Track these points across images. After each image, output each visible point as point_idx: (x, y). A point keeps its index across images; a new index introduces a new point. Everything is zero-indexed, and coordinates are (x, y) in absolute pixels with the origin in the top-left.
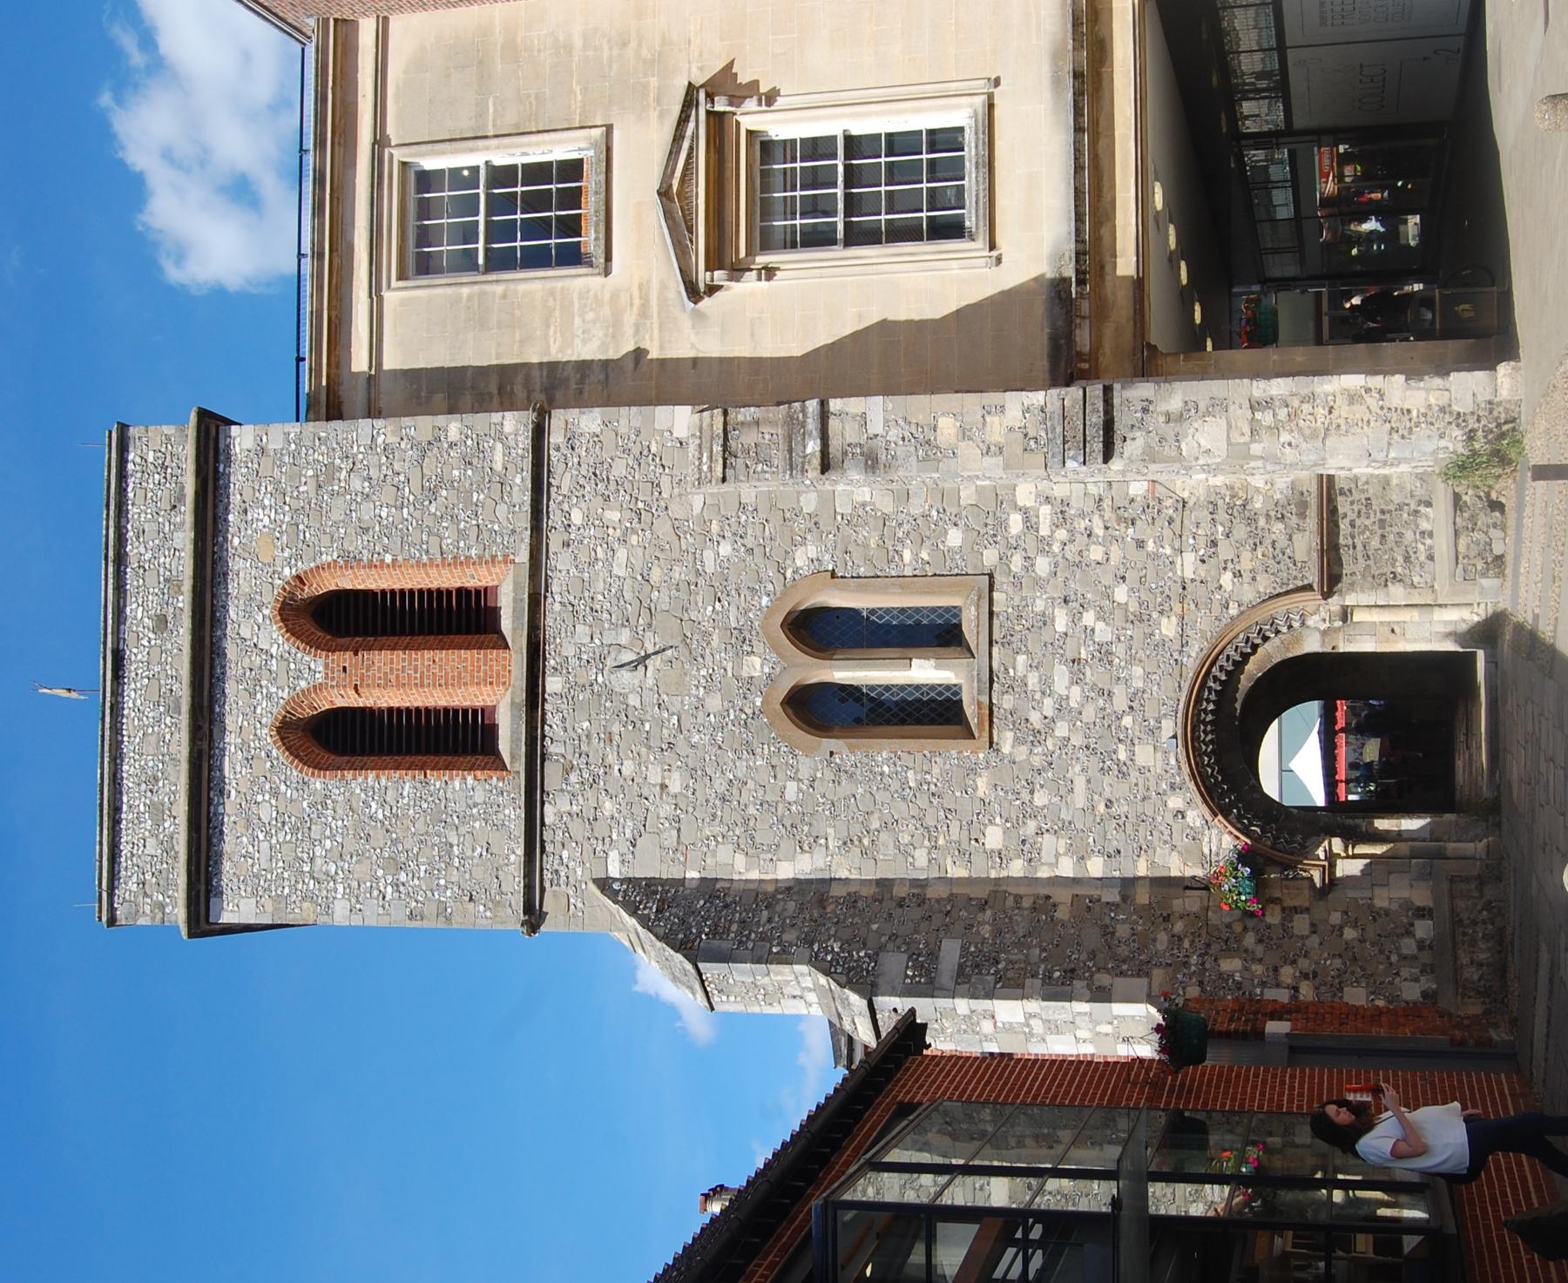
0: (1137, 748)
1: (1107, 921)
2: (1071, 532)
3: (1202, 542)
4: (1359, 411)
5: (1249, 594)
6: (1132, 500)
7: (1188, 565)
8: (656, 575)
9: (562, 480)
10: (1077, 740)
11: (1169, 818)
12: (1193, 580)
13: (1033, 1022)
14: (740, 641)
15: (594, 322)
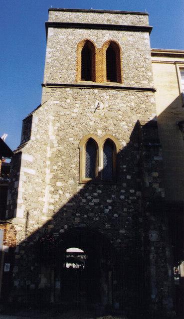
2: (130, 204)
8: (120, 112)
9: (139, 94)
10: (81, 204)
14: (105, 129)
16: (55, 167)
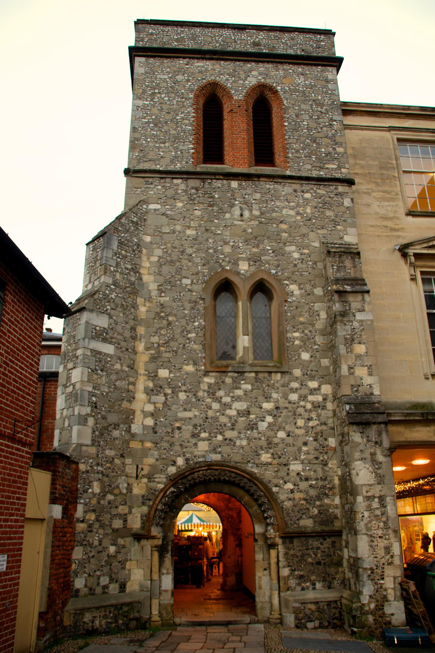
1: (122, 426)
2: (310, 411)
3: (307, 474)
4: (382, 552)
5: (282, 497)
6: (326, 440)
7: (296, 467)
8: (284, 226)
10: (210, 413)
12: (289, 469)
13: (71, 387)
14: (254, 260)
15: (387, 210)
16: (155, 339)
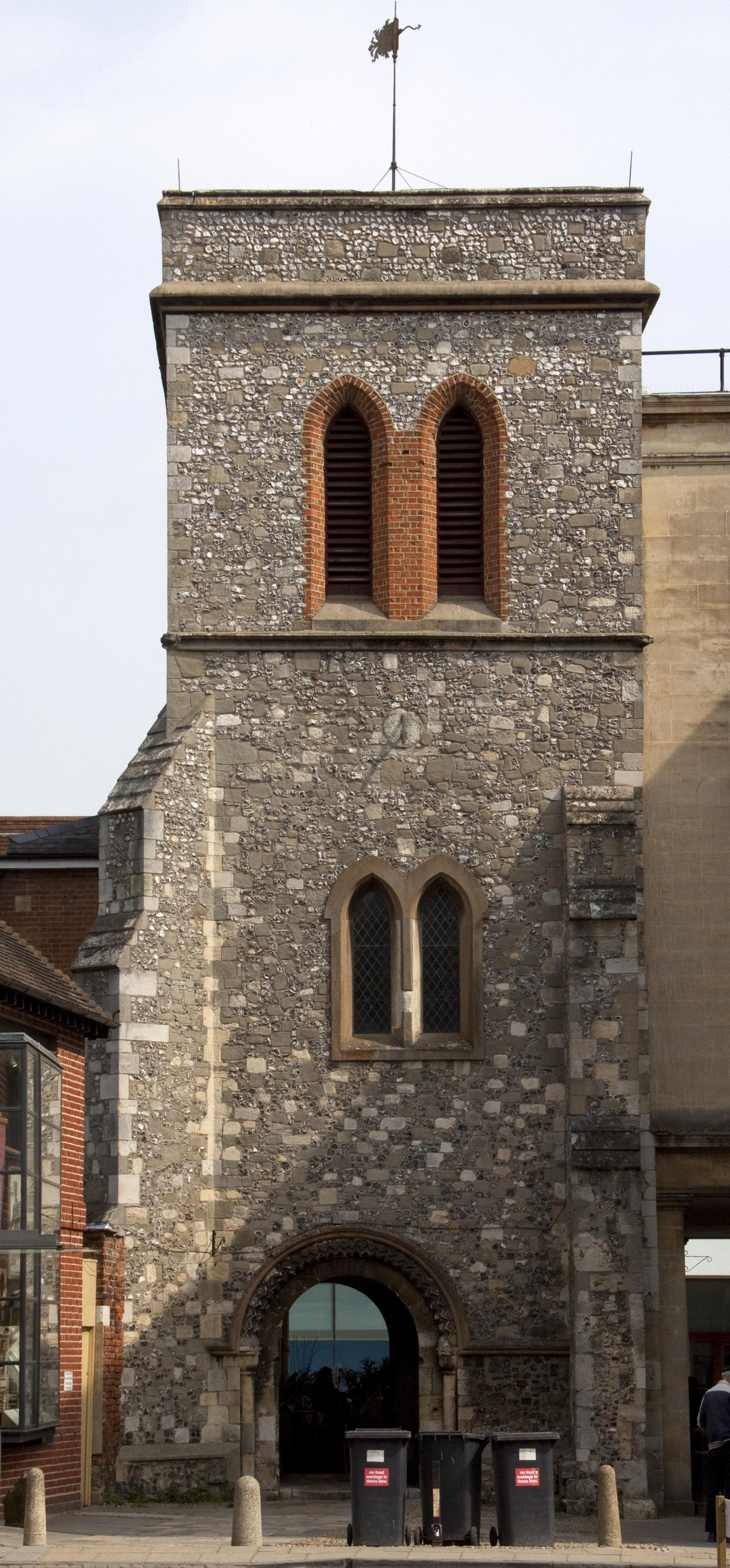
0: (334, 1190)
1: (186, 1166)
2: (522, 1132)
5: (467, 1286)
6: (549, 1185)
7: (492, 1234)
8: (491, 757)
10: (341, 1138)
11: (276, 1218)
12: (479, 1238)
13: (100, 1106)
14: (429, 833)
16: (240, 1001)
